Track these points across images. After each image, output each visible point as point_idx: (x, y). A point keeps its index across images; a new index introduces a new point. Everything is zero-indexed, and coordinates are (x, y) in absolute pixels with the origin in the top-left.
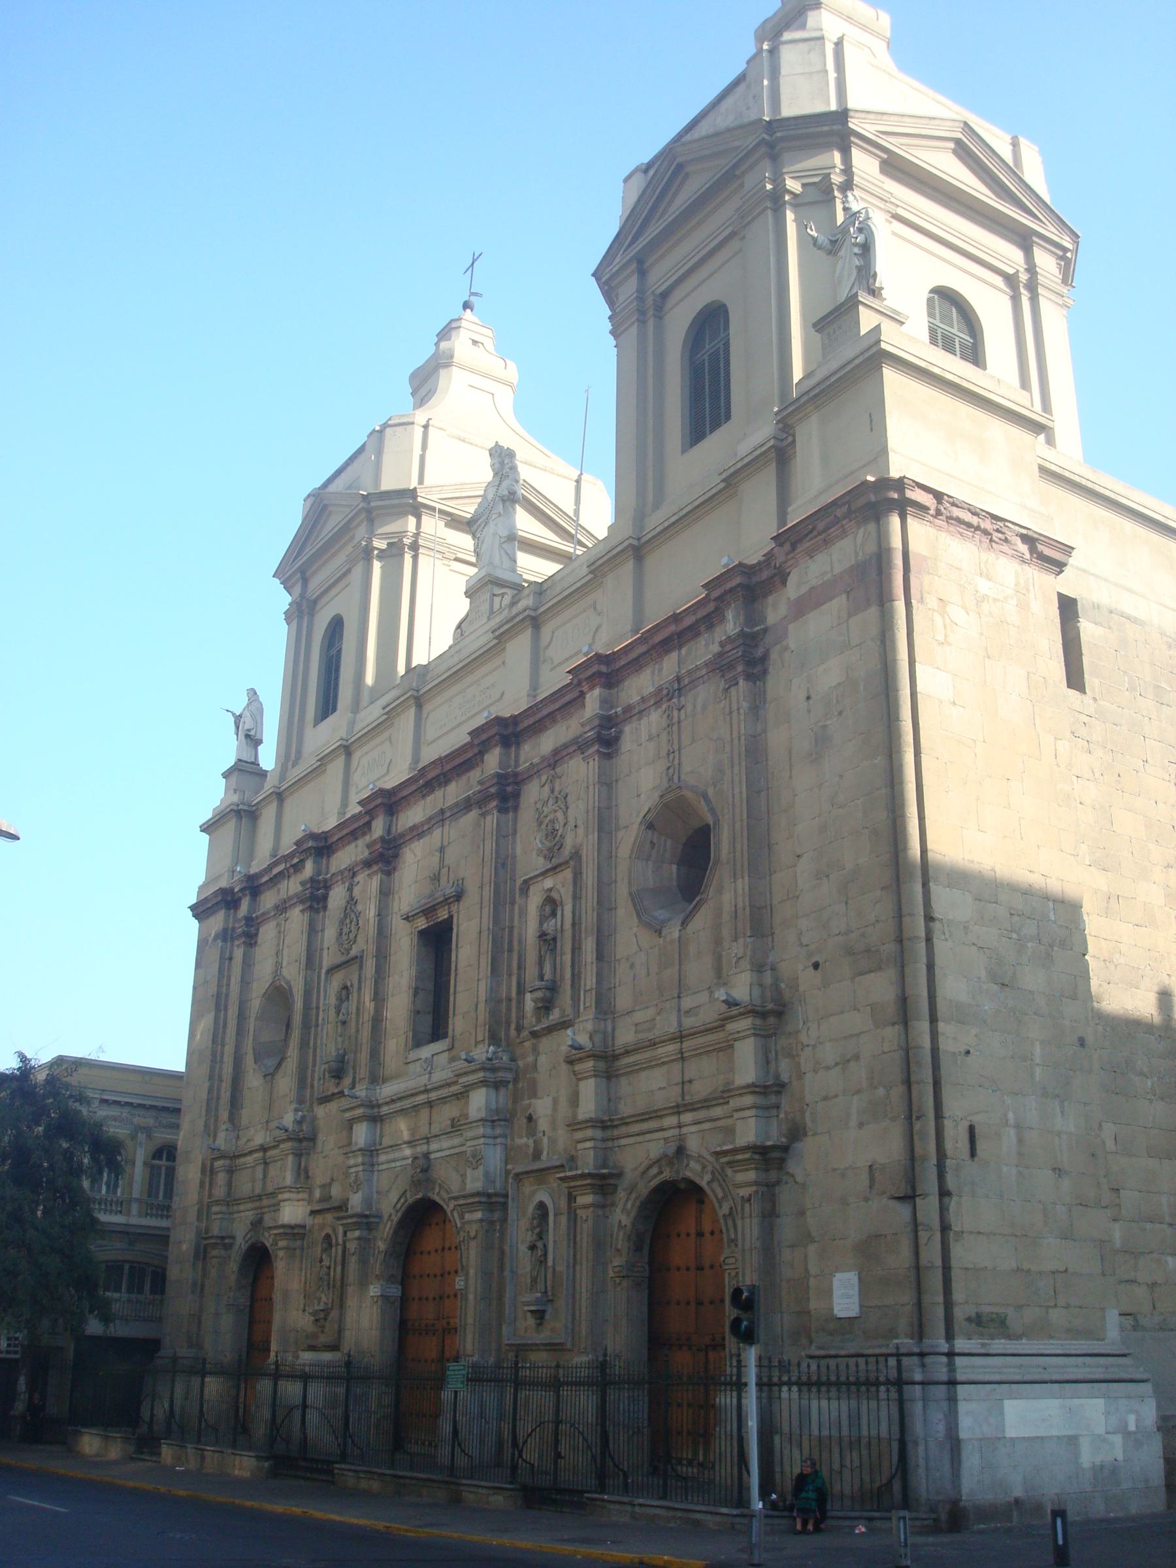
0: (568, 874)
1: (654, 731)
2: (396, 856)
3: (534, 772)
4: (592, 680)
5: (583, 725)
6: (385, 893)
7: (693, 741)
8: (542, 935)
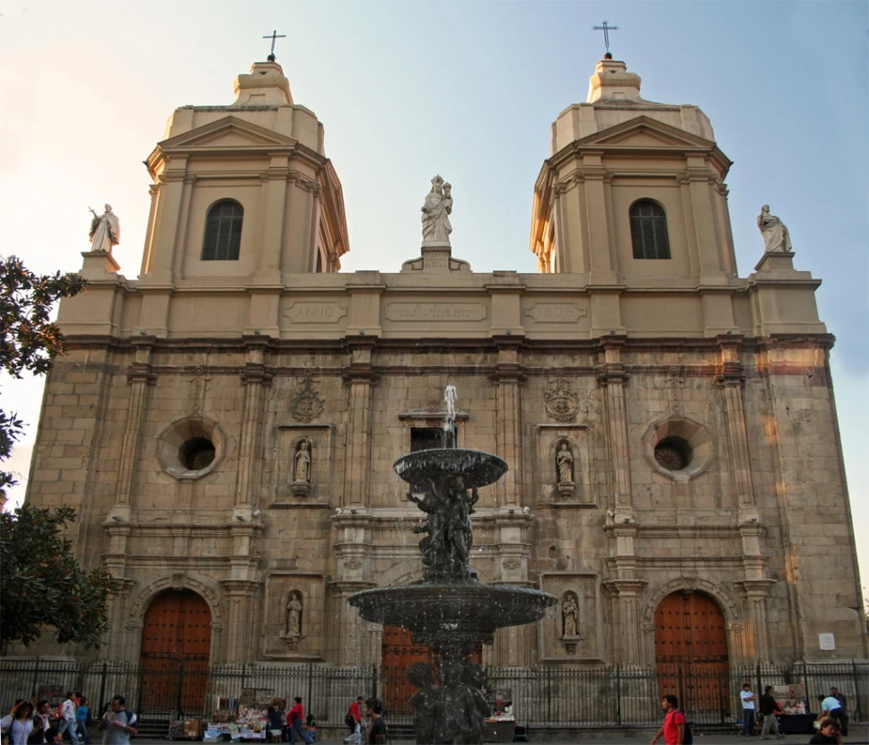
3: (538, 372)
4: (614, 346)
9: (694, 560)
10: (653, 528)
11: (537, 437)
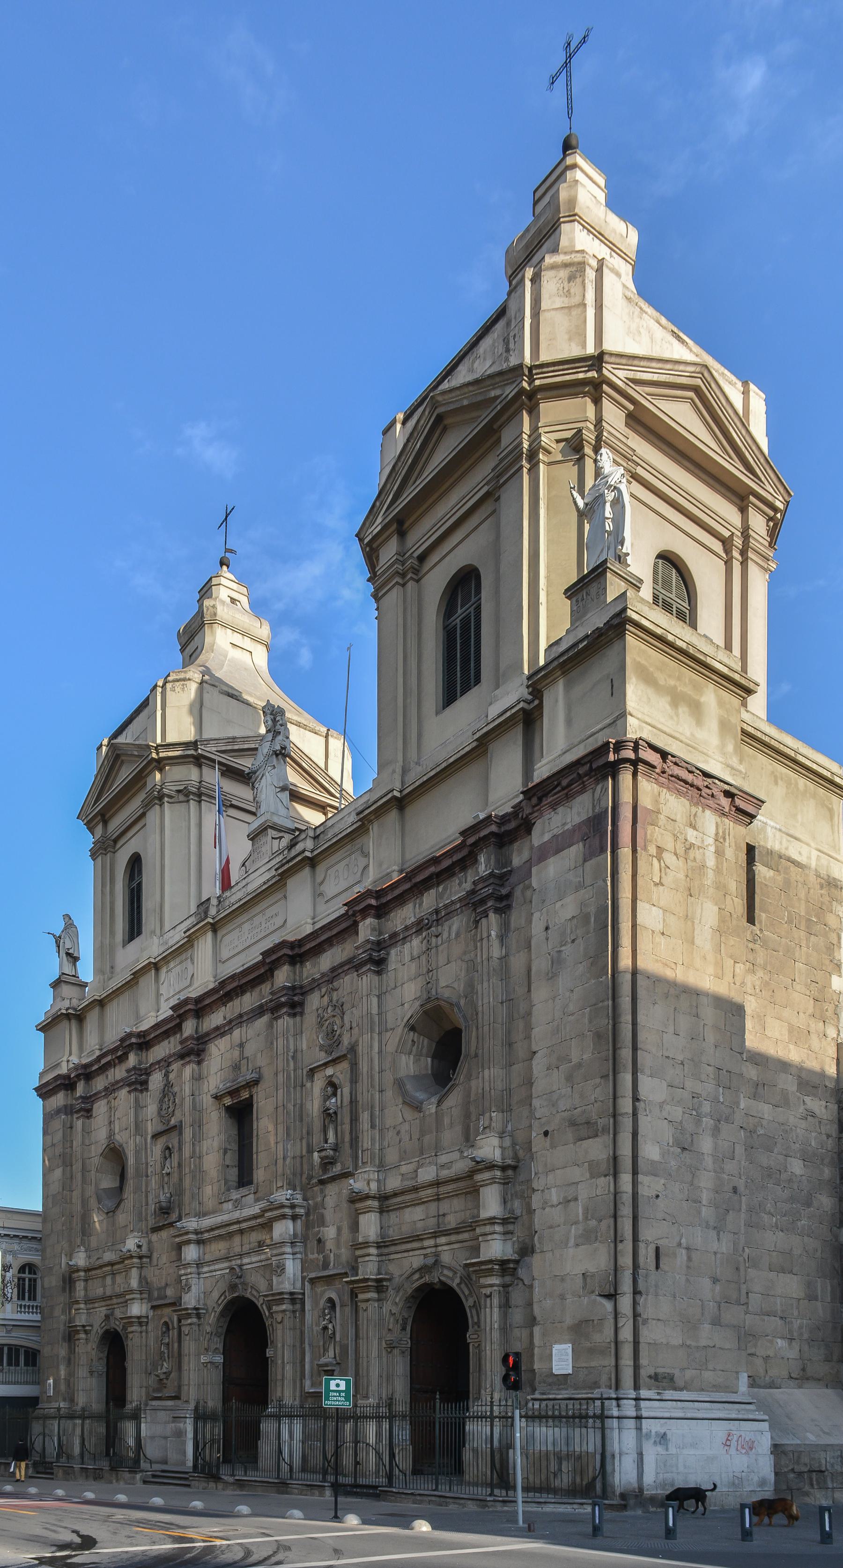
0: (345, 1065)
1: (415, 954)
2: (203, 1050)
4: (365, 912)
5: (357, 948)
6: (198, 1078)
7: (449, 962)
8: (326, 1112)
9: (435, 1235)
10: (395, 1195)
11: (309, 1085)
